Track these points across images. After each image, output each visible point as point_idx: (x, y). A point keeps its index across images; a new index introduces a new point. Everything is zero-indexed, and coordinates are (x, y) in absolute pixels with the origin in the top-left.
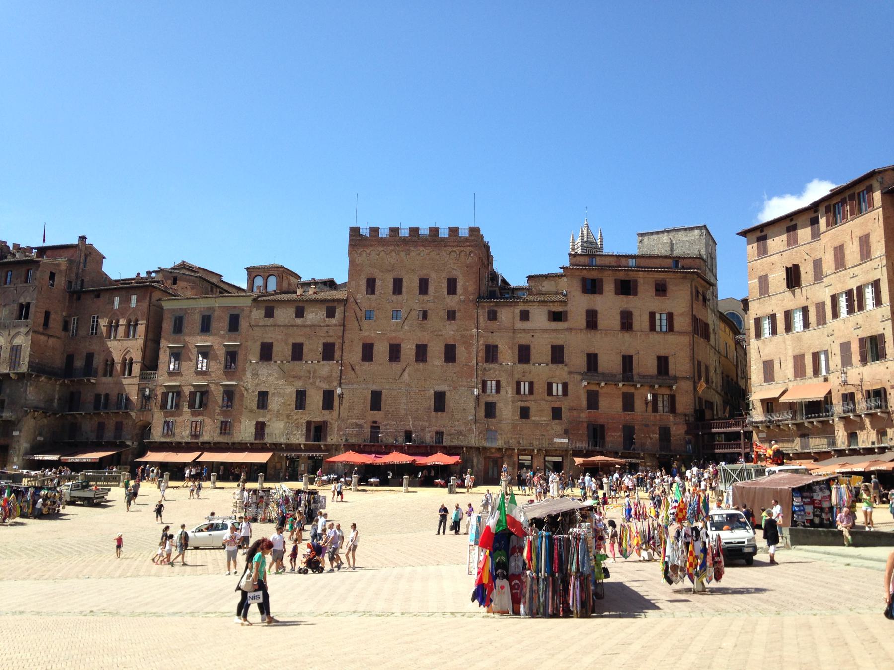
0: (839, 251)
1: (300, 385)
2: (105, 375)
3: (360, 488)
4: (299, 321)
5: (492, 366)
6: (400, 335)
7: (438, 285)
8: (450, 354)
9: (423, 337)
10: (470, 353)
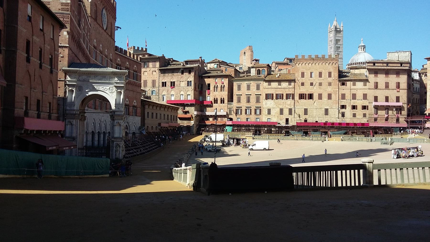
1: (281, 107)
2: (215, 103)
3: (303, 138)
4: (280, 87)
6: (313, 91)
7: (325, 74)
9: (320, 91)
10: (336, 96)
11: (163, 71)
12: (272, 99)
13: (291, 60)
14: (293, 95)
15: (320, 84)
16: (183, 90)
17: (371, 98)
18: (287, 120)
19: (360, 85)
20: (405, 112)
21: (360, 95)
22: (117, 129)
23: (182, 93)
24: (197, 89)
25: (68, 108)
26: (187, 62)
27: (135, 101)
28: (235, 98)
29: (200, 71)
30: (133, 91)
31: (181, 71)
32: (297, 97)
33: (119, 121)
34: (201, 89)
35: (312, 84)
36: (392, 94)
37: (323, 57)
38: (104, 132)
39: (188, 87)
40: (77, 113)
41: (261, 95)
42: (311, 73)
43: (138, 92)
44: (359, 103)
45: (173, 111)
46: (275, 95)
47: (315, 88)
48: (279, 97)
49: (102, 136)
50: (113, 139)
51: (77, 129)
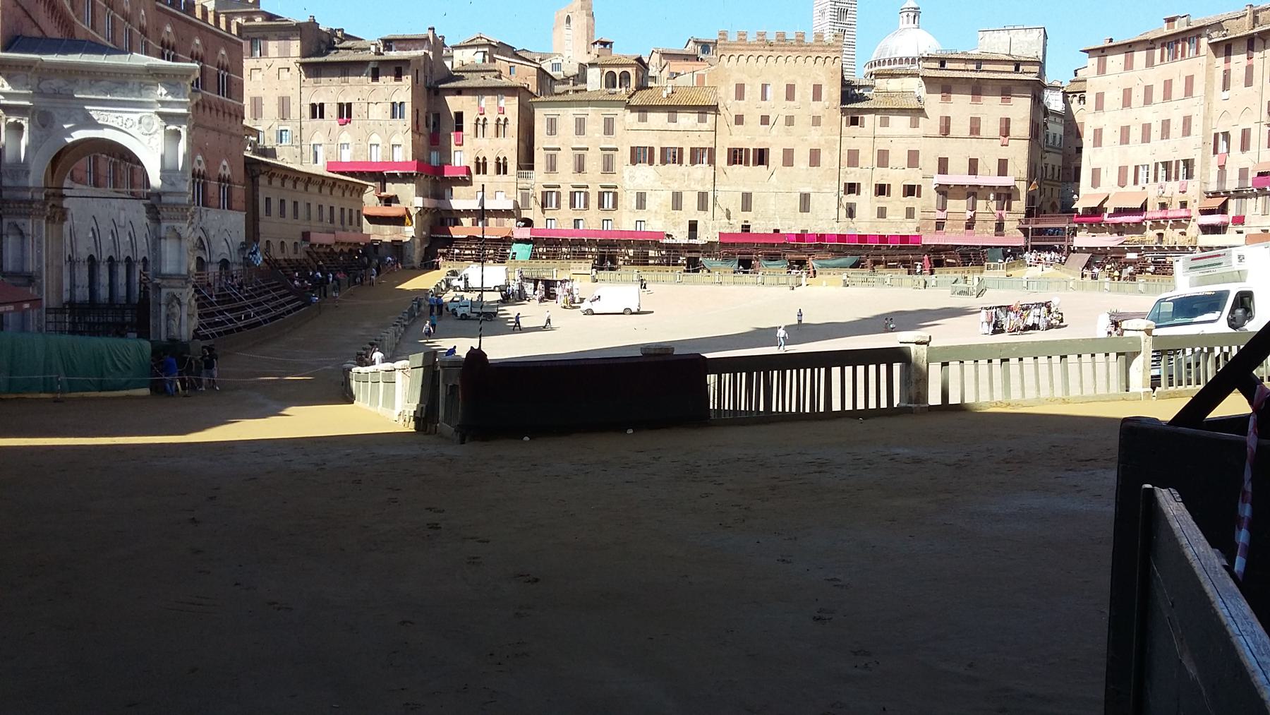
0: (1168, 85)
1: (676, 188)
2: (478, 173)
3: (737, 279)
4: (672, 126)
5: (853, 169)
7: (804, 92)
8: (815, 157)
11: (313, 70)
12: (651, 162)
13: (706, 47)
14: (712, 152)
15: (790, 121)
16: (379, 128)
17: (929, 163)
18: (693, 226)
19: (900, 123)
20: (1019, 205)
21: (898, 156)
22: (169, 250)
23: (375, 139)
24: (423, 129)
25: (6, 182)
26: (388, 43)
27: (225, 163)
28: (540, 158)
29: (431, 72)
30: (219, 131)
31: (369, 69)
32: (722, 158)
33: (177, 225)
34: (435, 128)
35: (765, 120)
36: (989, 153)
37: (800, 38)
38: (128, 259)
39: (393, 121)
40: (37, 196)
41: (616, 150)
42: (764, 87)
43: (232, 135)
44: (897, 177)
45: (347, 194)
46: (657, 153)
47: (774, 131)
48: (672, 156)
49: (122, 270)
50: (158, 281)
51: (40, 248)
